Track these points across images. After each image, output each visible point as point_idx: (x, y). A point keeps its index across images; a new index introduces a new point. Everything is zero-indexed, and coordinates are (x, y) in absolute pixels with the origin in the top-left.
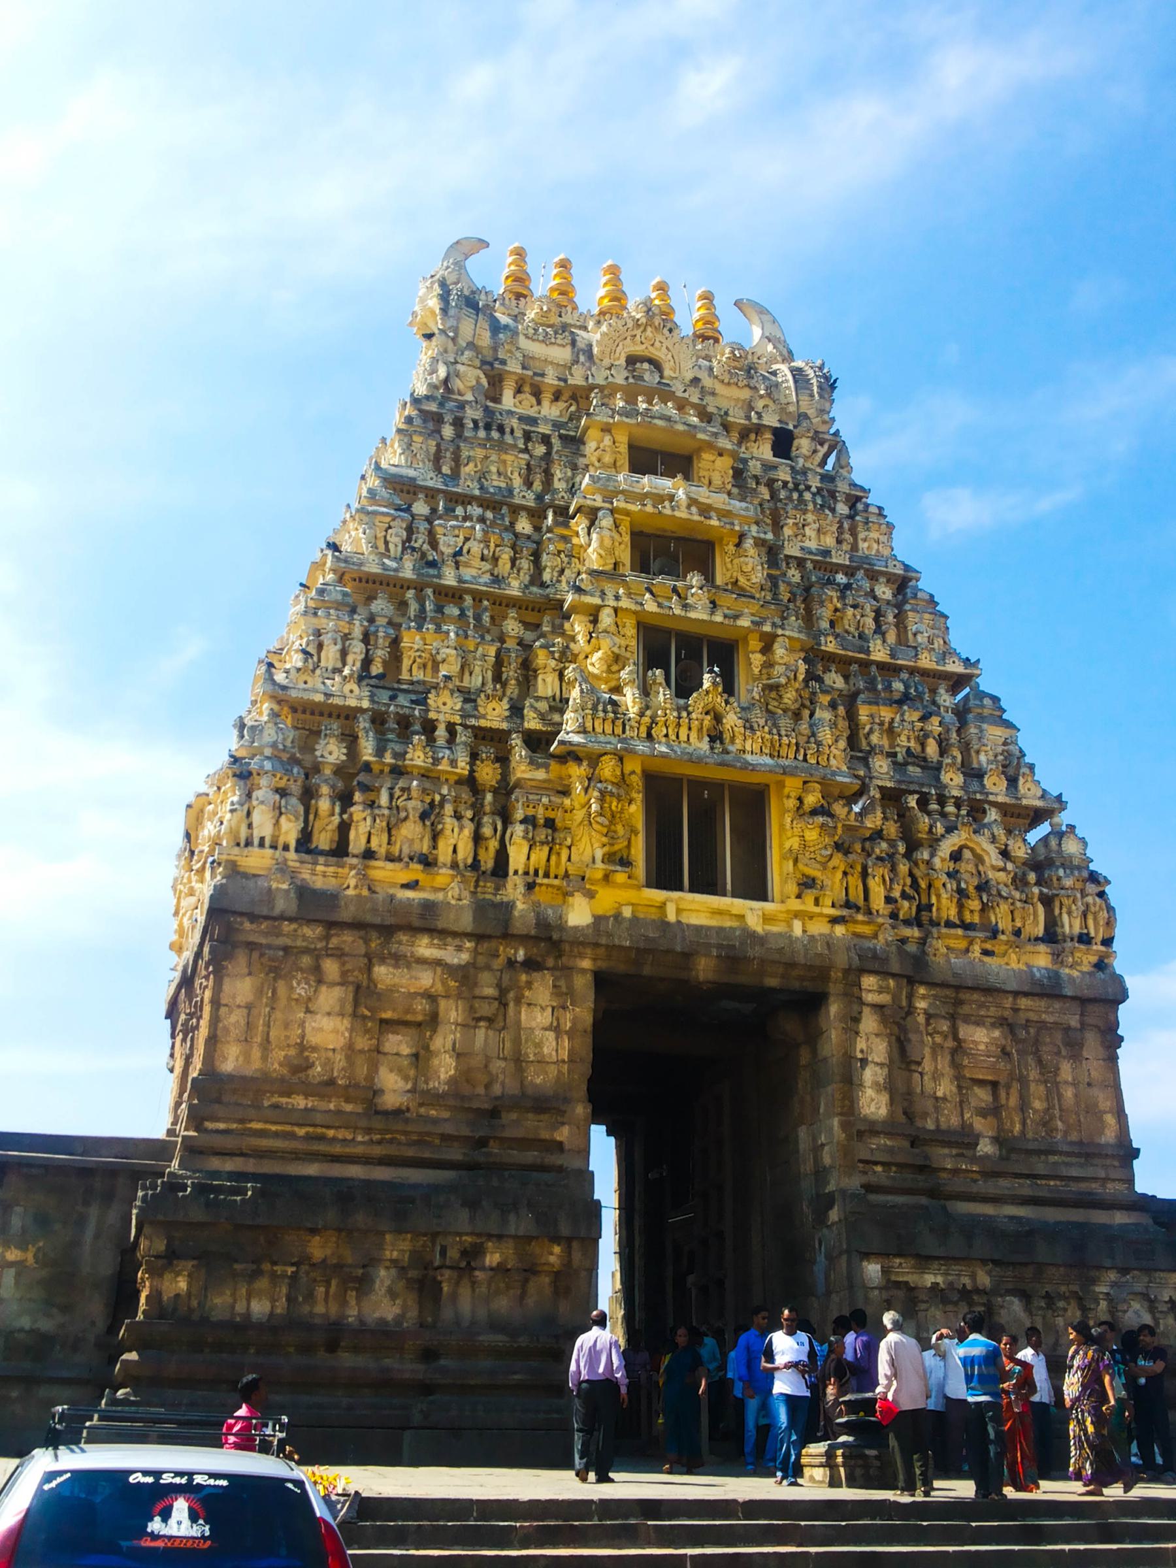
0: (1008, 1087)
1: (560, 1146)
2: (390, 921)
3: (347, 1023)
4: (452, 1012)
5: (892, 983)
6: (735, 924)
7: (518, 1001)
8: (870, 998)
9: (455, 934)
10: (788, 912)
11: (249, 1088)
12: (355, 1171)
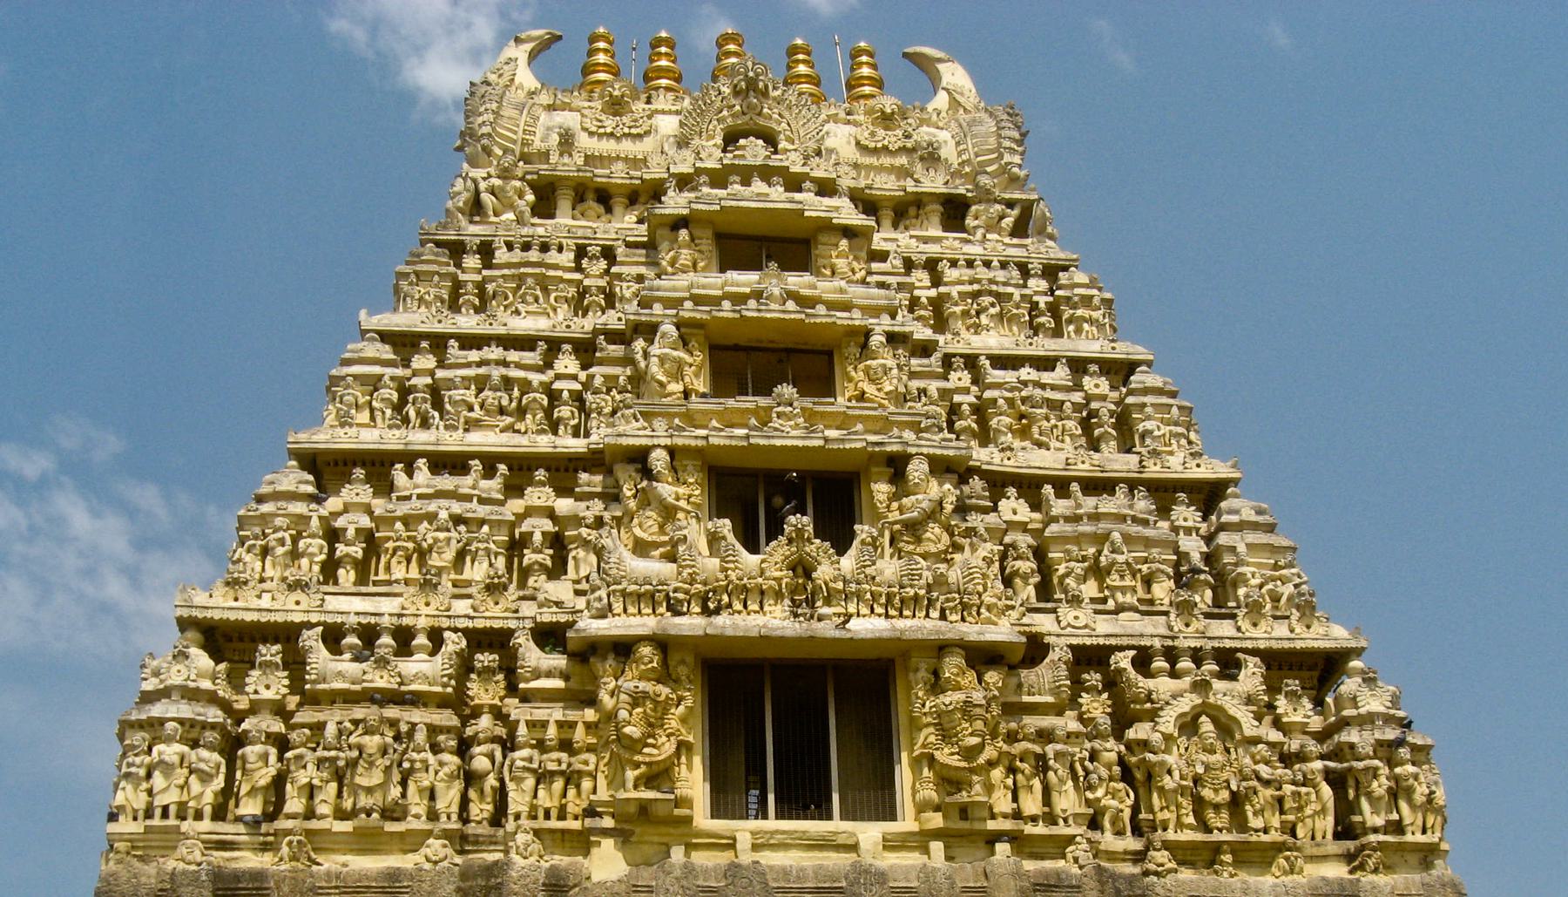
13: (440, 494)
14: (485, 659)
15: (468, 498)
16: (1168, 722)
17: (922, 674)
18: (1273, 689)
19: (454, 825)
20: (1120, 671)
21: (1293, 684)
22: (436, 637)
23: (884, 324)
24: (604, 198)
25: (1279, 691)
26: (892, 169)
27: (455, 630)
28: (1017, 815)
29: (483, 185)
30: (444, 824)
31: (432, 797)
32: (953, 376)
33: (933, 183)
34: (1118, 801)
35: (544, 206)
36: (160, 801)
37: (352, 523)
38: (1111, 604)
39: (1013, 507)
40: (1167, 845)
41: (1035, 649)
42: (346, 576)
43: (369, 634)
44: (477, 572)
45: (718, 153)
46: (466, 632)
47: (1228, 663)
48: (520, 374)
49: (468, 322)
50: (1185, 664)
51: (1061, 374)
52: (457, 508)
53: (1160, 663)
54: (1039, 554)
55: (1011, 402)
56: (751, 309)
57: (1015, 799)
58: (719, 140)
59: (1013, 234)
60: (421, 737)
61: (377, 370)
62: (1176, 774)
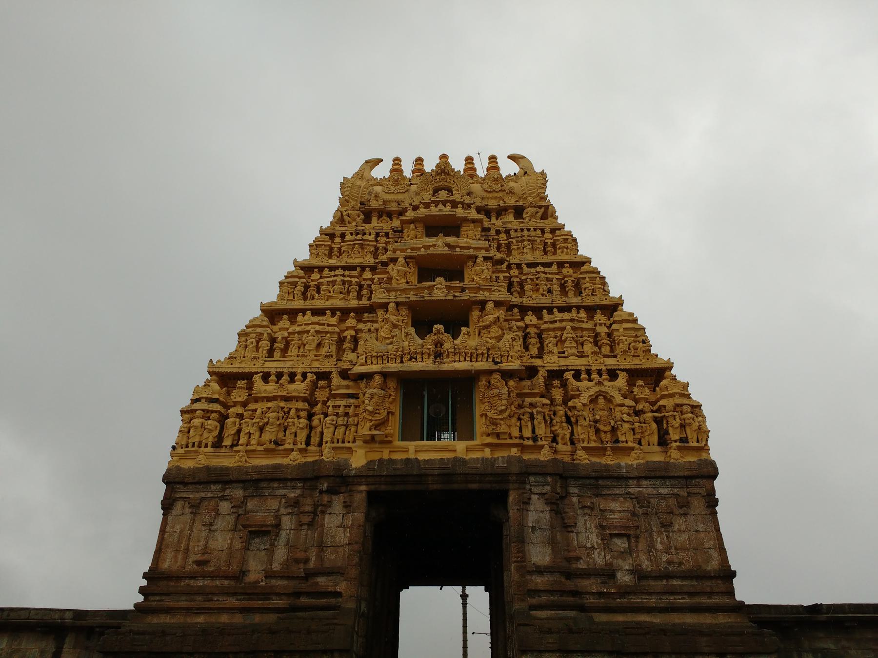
0: (637, 537)
1: (339, 594)
2: (256, 477)
3: (230, 535)
4: (287, 522)
5: (549, 479)
6: (450, 455)
7: (323, 512)
8: (535, 490)
9: (292, 480)
10: (482, 445)
11: (168, 577)
12: (224, 618)
13: (312, 323)
14: (321, 383)
15: (323, 324)
16: (585, 398)
17: (484, 382)
18: (631, 384)
19: (304, 446)
20: (567, 380)
21: (640, 382)
22: (304, 376)
23: (483, 253)
24: (390, 215)
25: (635, 385)
26: (495, 198)
27: (312, 373)
28: (521, 437)
29: (344, 214)
30: (299, 446)
31: (296, 436)
32: (512, 272)
33: (510, 201)
34: (564, 431)
35: (367, 220)
36: (191, 441)
37: (279, 335)
38: (566, 354)
39: (531, 319)
40: (584, 448)
41: (532, 371)
42: (277, 354)
43: (279, 375)
44: (324, 351)
45: (430, 196)
46: (316, 373)
47: (613, 375)
48: (348, 279)
49: (333, 261)
50: (595, 376)
51: (554, 268)
52: (318, 328)
53: (584, 376)
54: (539, 336)
55: (532, 279)
56: (432, 250)
57: (521, 430)
58: (431, 192)
59: (541, 219)
60: (293, 412)
61: (297, 280)
62: (587, 419)
